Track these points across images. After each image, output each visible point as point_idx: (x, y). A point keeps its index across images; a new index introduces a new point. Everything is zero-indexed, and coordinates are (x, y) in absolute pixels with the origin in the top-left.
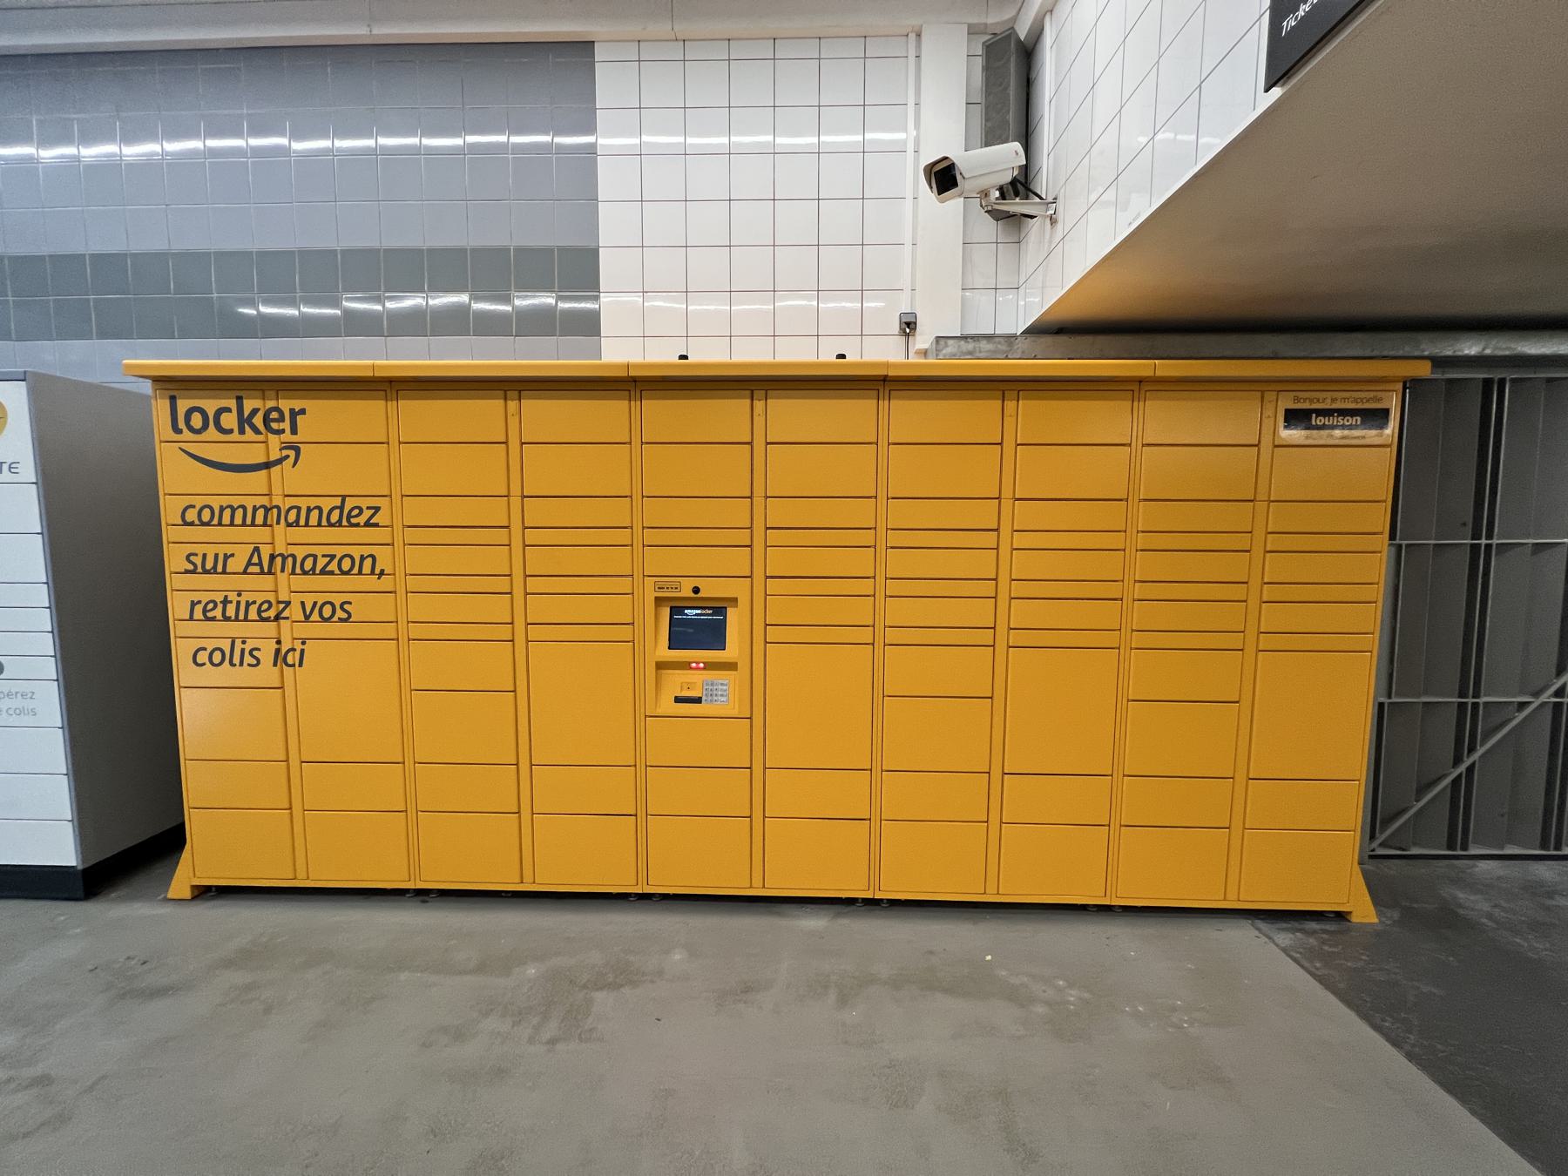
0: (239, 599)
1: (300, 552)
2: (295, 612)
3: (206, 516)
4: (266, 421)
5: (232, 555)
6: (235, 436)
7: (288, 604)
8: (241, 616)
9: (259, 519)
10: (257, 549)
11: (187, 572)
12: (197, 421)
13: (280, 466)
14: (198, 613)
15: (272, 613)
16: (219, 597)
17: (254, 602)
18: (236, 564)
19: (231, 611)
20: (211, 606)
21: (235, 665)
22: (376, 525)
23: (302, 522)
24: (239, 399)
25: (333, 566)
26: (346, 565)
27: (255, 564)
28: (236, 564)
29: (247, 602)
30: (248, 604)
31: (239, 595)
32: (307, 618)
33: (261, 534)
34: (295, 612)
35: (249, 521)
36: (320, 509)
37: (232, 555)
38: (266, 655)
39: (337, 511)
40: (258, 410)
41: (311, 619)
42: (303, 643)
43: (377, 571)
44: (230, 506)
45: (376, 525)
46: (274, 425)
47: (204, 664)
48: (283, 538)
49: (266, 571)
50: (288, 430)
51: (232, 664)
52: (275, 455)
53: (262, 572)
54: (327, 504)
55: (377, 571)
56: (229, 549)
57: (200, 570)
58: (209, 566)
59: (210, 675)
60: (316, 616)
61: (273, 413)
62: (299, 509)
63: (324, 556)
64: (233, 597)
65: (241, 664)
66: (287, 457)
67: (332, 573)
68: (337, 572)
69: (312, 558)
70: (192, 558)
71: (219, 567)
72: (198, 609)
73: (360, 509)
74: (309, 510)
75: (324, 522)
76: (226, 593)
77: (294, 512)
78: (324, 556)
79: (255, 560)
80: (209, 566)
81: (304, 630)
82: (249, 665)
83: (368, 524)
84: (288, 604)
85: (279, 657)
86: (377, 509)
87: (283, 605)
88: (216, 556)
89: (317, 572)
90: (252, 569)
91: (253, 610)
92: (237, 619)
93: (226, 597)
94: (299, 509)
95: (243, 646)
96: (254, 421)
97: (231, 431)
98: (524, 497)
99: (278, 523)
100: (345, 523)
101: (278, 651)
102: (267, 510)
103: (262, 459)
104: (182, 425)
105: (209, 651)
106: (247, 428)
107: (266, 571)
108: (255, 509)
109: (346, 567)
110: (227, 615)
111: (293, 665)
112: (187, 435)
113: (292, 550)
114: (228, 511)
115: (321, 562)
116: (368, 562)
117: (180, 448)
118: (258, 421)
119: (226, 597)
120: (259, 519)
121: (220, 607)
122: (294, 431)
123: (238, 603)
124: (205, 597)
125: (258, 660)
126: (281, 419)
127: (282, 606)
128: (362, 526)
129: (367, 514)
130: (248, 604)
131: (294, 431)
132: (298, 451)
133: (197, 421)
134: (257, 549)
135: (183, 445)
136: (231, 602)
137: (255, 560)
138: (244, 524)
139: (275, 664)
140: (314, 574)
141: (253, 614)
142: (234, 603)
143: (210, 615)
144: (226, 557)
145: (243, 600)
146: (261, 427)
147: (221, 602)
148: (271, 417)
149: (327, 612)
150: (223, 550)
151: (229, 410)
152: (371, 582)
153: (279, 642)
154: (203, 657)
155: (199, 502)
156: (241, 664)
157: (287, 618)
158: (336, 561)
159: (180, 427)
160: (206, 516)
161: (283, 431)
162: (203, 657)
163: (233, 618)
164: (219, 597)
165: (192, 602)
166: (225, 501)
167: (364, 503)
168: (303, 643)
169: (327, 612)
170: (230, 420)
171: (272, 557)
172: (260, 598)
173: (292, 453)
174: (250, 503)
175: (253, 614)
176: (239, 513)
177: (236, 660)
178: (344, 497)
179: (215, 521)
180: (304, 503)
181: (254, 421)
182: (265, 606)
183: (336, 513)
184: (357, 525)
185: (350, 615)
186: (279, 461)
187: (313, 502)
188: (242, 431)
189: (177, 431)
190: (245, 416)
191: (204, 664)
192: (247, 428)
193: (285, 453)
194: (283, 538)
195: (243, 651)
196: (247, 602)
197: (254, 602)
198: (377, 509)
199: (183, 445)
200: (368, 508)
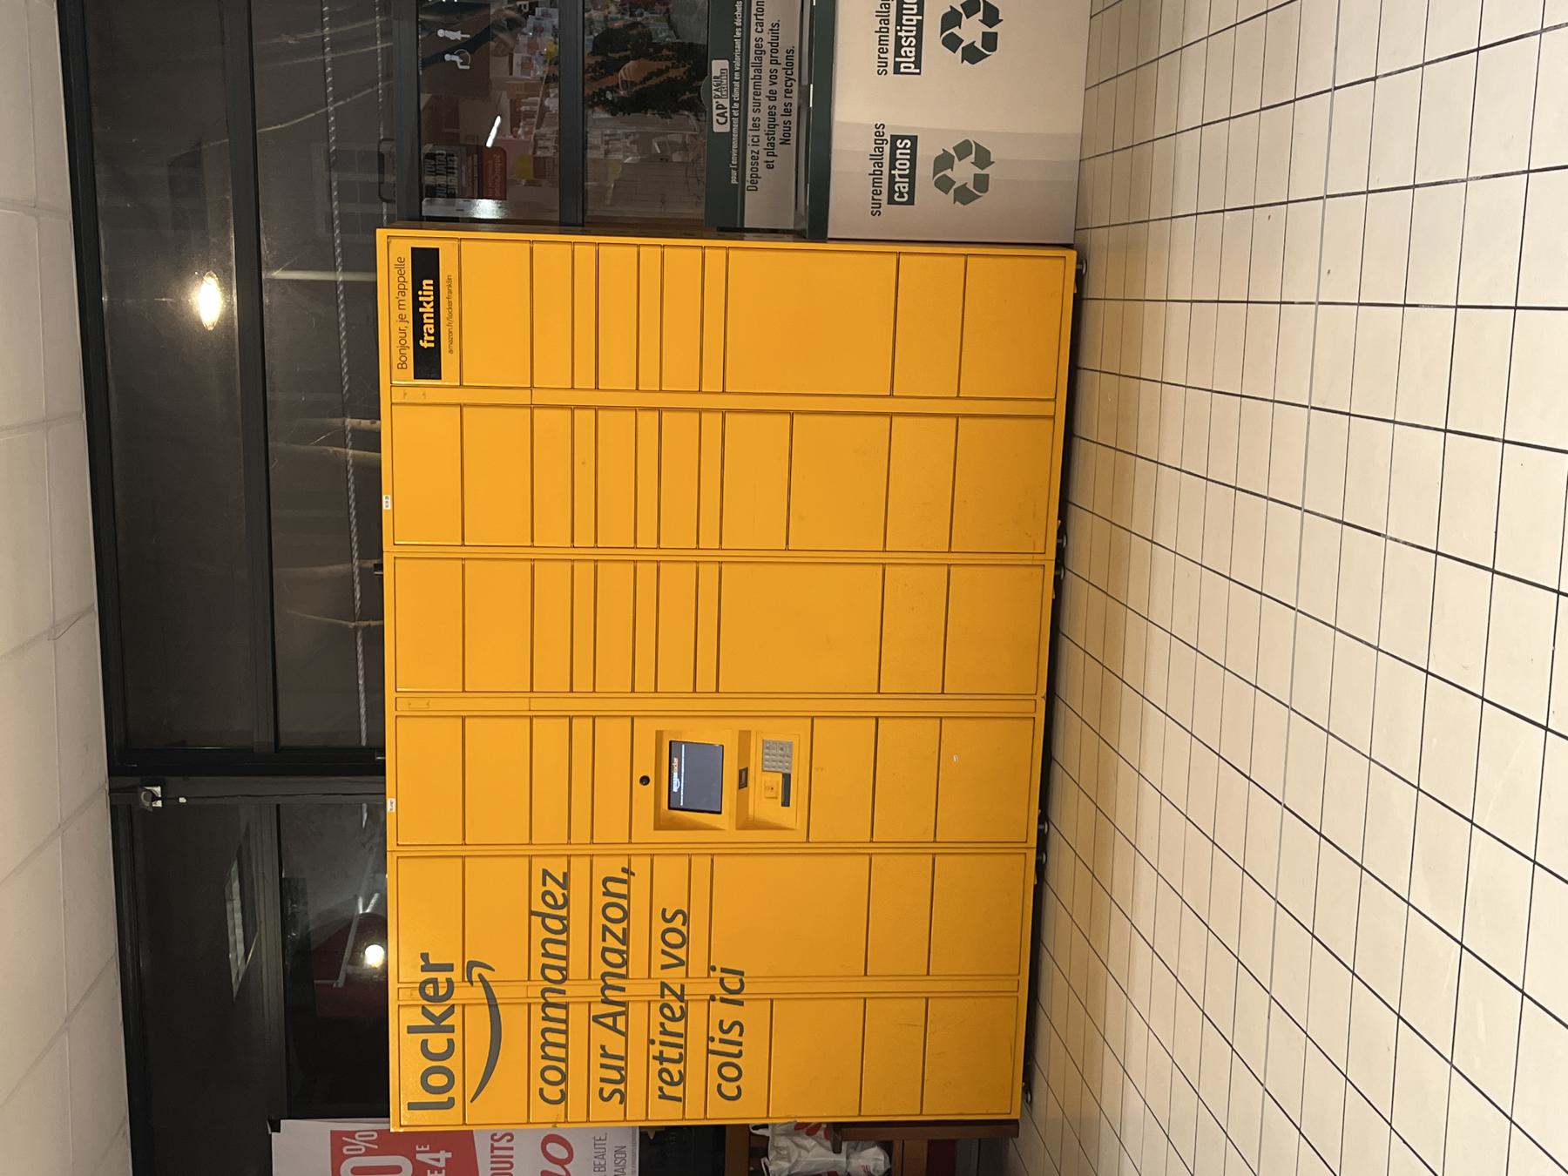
0: (657, 1043)
1: (600, 967)
2: (675, 976)
3: (553, 1076)
4: (436, 999)
5: (603, 1048)
6: (456, 1036)
7: (664, 985)
9: (560, 1014)
10: (596, 1019)
11: (623, 1100)
12: (437, 1080)
14: (676, 1091)
15: (676, 1006)
16: (655, 1066)
17: (662, 1025)
18: (615, 1044)
19: (672, 1053)
20: (665, 1076)
21: (741, 1052)
22: (566, 875)
23: (562, 964)
25: (618, 929)
26: (615, 913)
27: (615, 1022)
28: (615, 1044)
29: (661, 1033)
30: (664, 1032)
31: (653, 1042)
32: (681, 963)
33: (578, 1015)
34: (675, 976)
35: (563, 1027)
36: (544, 942)
37: (603, 1048)
38: (728, 1013)
39: (548, 921)
41: (685, 959)
42: (714, 969)
43: (625, 876)
44: (543, 1047)
45: (566, 875)
46: (442, 992)
47: (738, 1088)
48: (582, 988)
49: (621, 1009)
51: (740, 1055)
52: (478, 992)
53: (625, 1013)
54: (540, 934)
55: (625, 876)
56: (596, 1052)
57: (621, 1087)
58: (615, 1076)
59: (752, 1082)
60: (680, 953)
61: (427, 992)
62: (545, 967)
63: (604, 940)
64: (655, 1050)
65: (740, 1044)
66: (480, 975)
67: (626, 932)
68: (624, 924)
69: (607, 954)
70: (606, 1095)
71: (617, 1065)
72: (668, 1090)
73: (545, 894)
74: (546, 955)
75: (563, 937)
77: (548, 973)
78: (604, 940)
79: (609, 1021)
80: (615, 1076)
81: (698, 965)
82: (741, 1035)
83: (565, 885)
84: (664, 985)
85: (733, 998)
86: (546, 873)
87: (666, 990)
88: (603, 1066)
89: (624, 948)
90: (621, 1025)
91: (670, 1026)
93: (654, 1058)
94: (545, 967)
95: (717, 1040)
96: (437, 1015)
99: (563, 992)
100: (563, 913)
101: (723, 1000)
102: (547, 1004)
103: (485, 1011)
104: (443, 1098)
105: (721, 1081)
107: (624, 1009)
108: (547, 1018)
109: (618, 914)
110: (677, 1057)
111: (741, 981)
112: (455, 1092)
113: (596, 974)
114: (547, 1049)
115: (612, 942)
116: (612, 887)
117: (472, 1101)
118: (437, 1011)
119: (654, 1058)
120: (560, 1014)
121: (666, 1065)
123: (662, 1043)
124: (655, 1082)
125: (734, 1023)
126: (435, 982)
127: (666, 992)
128: (569, 892)
129: (551, 886)
132: (473, 964)
133: (437, 1080)
134: (596, 1019)
135: (470, 1095)
136: (661, 1052)
137: (609, 1021)
138: (565, 1032)
139: (740, 1003)
140: (627, 952)
141: (677, 1027)
142: (662, 1048)
143: (676, 1078)
144: (605, 1055)
145: (658, 1038)
147: (661, 1064)
148: (432, 994)
149: (674, 938)
150: (597, 1059)
151: (424, 1043)
152: (639, 884)
153: (713, 998)
154: (729, 1089)
155: (537, 1083)
156: (740, 1044)
157: (682, 987)
158: (609, 924)
160: (553, 1076)
161: (449, 981)
162: (729, 1089)
163: (682, 1051)
164: (655, 1066)
165: (660, 1097)
166: (536, 1053)
167: (538, 889)
168: (714, 969)
169: (674, 938)
170: (438, 1043)
171: (606, 1001)
172: (657, 1018)
174: (538, 1024)
175: (677, 1027)
176: (550, 1037)
177: (734, 1049)
178: (532, 913)
179: (562, 1066)
180: (538, 961)
182: (667, 1012)
183: (551, 923)
184: (566, 900)
185: (679, 912)
187: (537, 950)
188: (451, 1029)
189: (450, 1104)
190: (432, 1024)
191: (738, 1088)
194: (582, 988)
195: (721, 1041)
197: (662, 1025)
198: (546, 873)
199: (468, 1101)
200: (544, 884)
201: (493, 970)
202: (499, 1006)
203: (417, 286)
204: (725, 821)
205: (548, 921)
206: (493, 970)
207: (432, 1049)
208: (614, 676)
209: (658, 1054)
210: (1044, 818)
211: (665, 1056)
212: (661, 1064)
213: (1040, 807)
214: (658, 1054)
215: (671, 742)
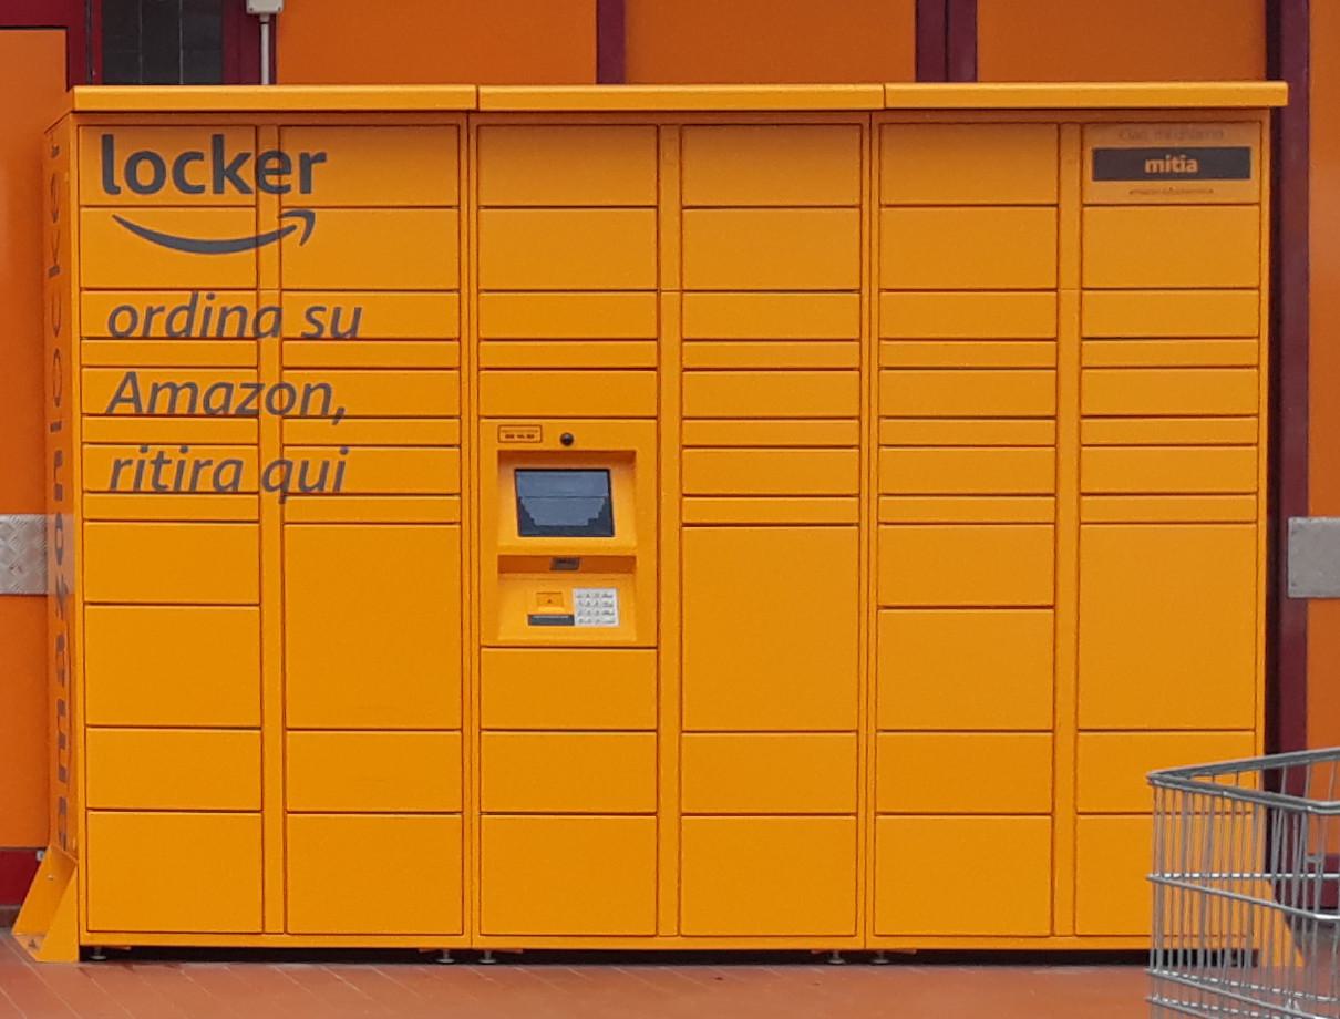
0: (182, 457)
6: (208, 196)
8: (185, 486)
12: (145, 173)
13: (276, 243)
19: (167, 478)
24: (218, 143)
29: (197, 462)
30: (198, 466)
31: (184, 451)
40: (248, 155)
46: (272, 180)
52: (269, 225)
61: (271, 161)
64: (172, 453)
66: (293, 228)
76: (160, 448)
92: (177, 491)
93: (161, 454)
97: (201, 189)
104: (119, 179)
106: (227, 182)
110: (161, 483)
117: (114, 217)
118: (247, 173)
119: (161, 454)
122: (306, 188)
123: (182, 463)
130: (198, 466)
131: (306, 188)
133: (145, 173)
136: (169, 462)
146: (252, 185)
147: (152, 462)
159: (117, 183)
161: (288, 188)
175: (205, 482)
181: (240, 173)
186: (279, 235)
188: (218, 189)
189: (111, 188)
192: (227, 182)
193: (287, 222)
196: (197, 462)
201: (302, 244)
202: (253, 251)
204: (511, 539)
206: (302, 244)
207: (190, 166)
208: (705, 393)
209: (166, 457)
211: (164, 467)
212: (152, 462)
214: (166, 457)
215: (608, 471)
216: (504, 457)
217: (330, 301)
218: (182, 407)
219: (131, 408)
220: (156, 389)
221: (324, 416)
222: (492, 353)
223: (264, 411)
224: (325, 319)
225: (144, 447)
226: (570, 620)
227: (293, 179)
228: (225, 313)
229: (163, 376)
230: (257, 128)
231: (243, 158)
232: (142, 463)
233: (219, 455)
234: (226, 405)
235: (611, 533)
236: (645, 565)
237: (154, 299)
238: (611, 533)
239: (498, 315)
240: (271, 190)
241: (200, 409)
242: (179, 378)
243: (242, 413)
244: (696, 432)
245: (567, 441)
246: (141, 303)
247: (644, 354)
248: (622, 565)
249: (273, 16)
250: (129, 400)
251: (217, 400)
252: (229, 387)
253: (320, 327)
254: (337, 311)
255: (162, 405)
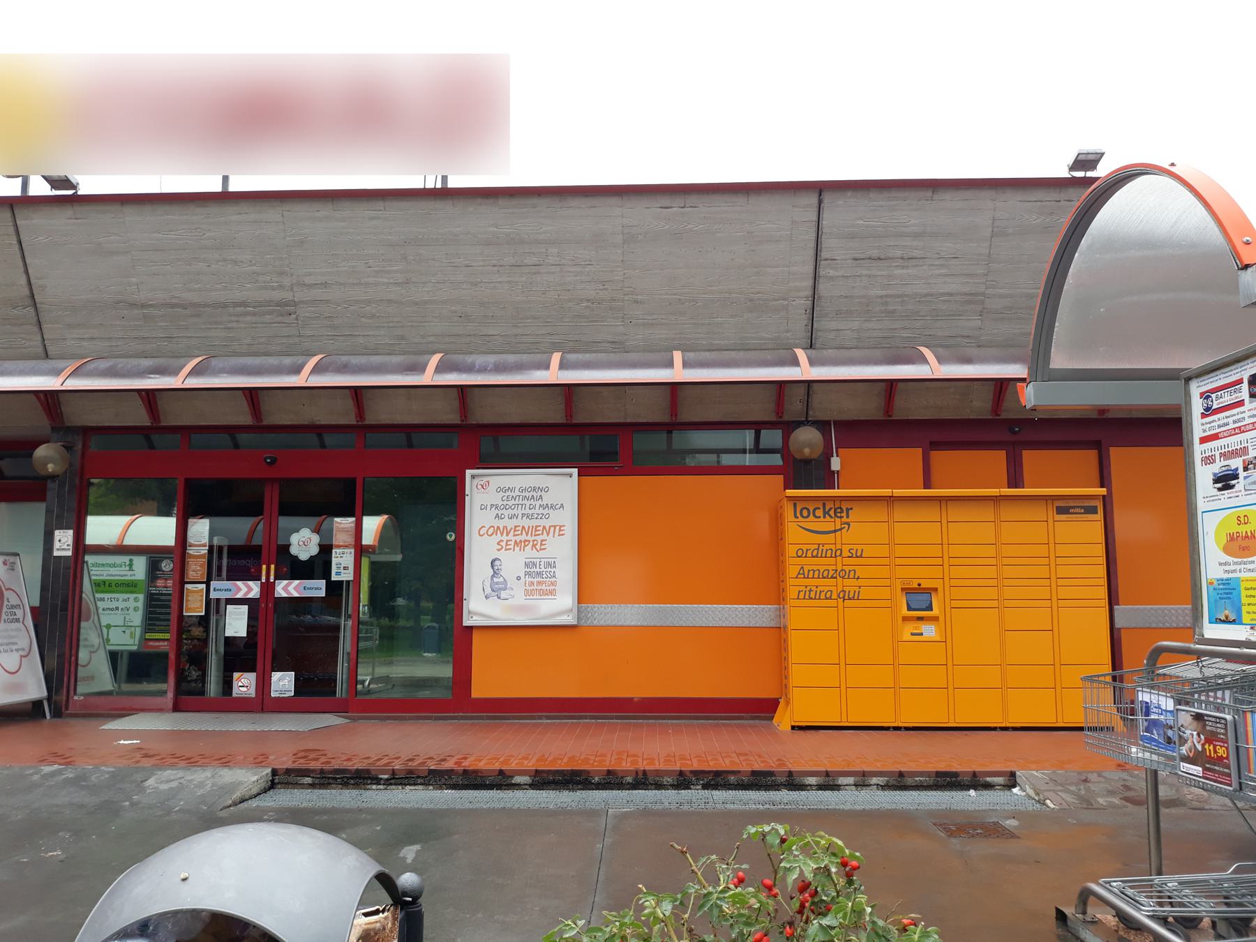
6: (822, 519)
8: (817, 598)
19: (812, 595)
24: (824, 505)
30: (821, 592)
46: (839, 515)
50: (845, 517)
64: (813, 588)
91: (823, 594)
93: (811, 589)
97: (820, 517)
98: (949, 544)
104: (798, 515)
110: (811, 596)
112: (800, 519)
118: (832, 513)
119: (811, 589)
132: (849, 525)
146: (833, 516)
161: (841, 517)
170: (819, 513)
173: (846, 526)
186: (841, 529)
188: (824, 517)
193: (843, 526)
203: (1082, 507)
204: (905, 612)
205: (816, 551)
207: (817, 511)
210: (907, 729)
213: (914, 727)
216: (903, 589)
217: (855, 547)
218: (816, 576)
219: (802, 576)
220: (809, 571)
221: (854, 578)
222: (898, 561)
223: (838, 577)
224: (854, 552)
225: (806, 587)
226: (922, 634)
227: (844, 514)
228: (827, 550)
229: (811, 568)
230: (834, 501)
231: (831, 509)
232: (806, 591)
233: (826, 589)
234: (828, 576)
235: (932, 610)
236: (942, 619)
237: (808, 547)
238: (932, 610)
239: (900, 551)
240: (838, 517)
241: (821, 577)
242: (815, 568)
243: (832, 577)
244: (954, 582)
245: (919, 585)
246: (805, 548)
247: (939, 561)
248: (935, 619)
249: (838, 471)
250: (802, 574)
251: (825, 574)
252: (828, 570)
253: (853, 554)
254: (857, 550)
255: (811, 576)
